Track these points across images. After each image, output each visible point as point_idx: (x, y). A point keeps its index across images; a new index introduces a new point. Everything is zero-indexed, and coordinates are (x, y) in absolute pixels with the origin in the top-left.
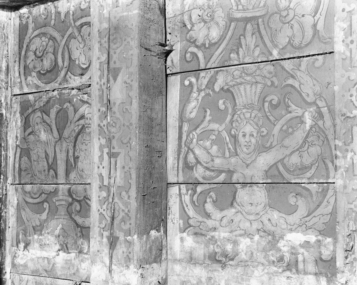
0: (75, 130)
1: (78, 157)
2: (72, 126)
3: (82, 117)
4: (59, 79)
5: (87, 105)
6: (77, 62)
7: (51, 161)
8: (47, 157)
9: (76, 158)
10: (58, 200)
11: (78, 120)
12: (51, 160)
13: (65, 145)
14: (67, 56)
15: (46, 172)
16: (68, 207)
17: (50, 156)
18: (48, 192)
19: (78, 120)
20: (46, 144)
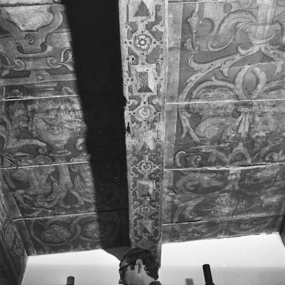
0: (54, 195)
1: (47, 181)
2: (58, 197)
3: (49, 202)
4: (78, 219)
5: (47, 207)
6: (62, 228)
7: (78, 178)
8: (82, 179)
9: (48, 180)
10: (66, 153)
11: (52, 201)
12: (78, 178)
13: (63, 187)
14: (72, 230)
15: (82, 170)
16: (52, 150)
17: (78, 180)
18: (79, 157)
19: (52, 201)
20: (84, 186)
